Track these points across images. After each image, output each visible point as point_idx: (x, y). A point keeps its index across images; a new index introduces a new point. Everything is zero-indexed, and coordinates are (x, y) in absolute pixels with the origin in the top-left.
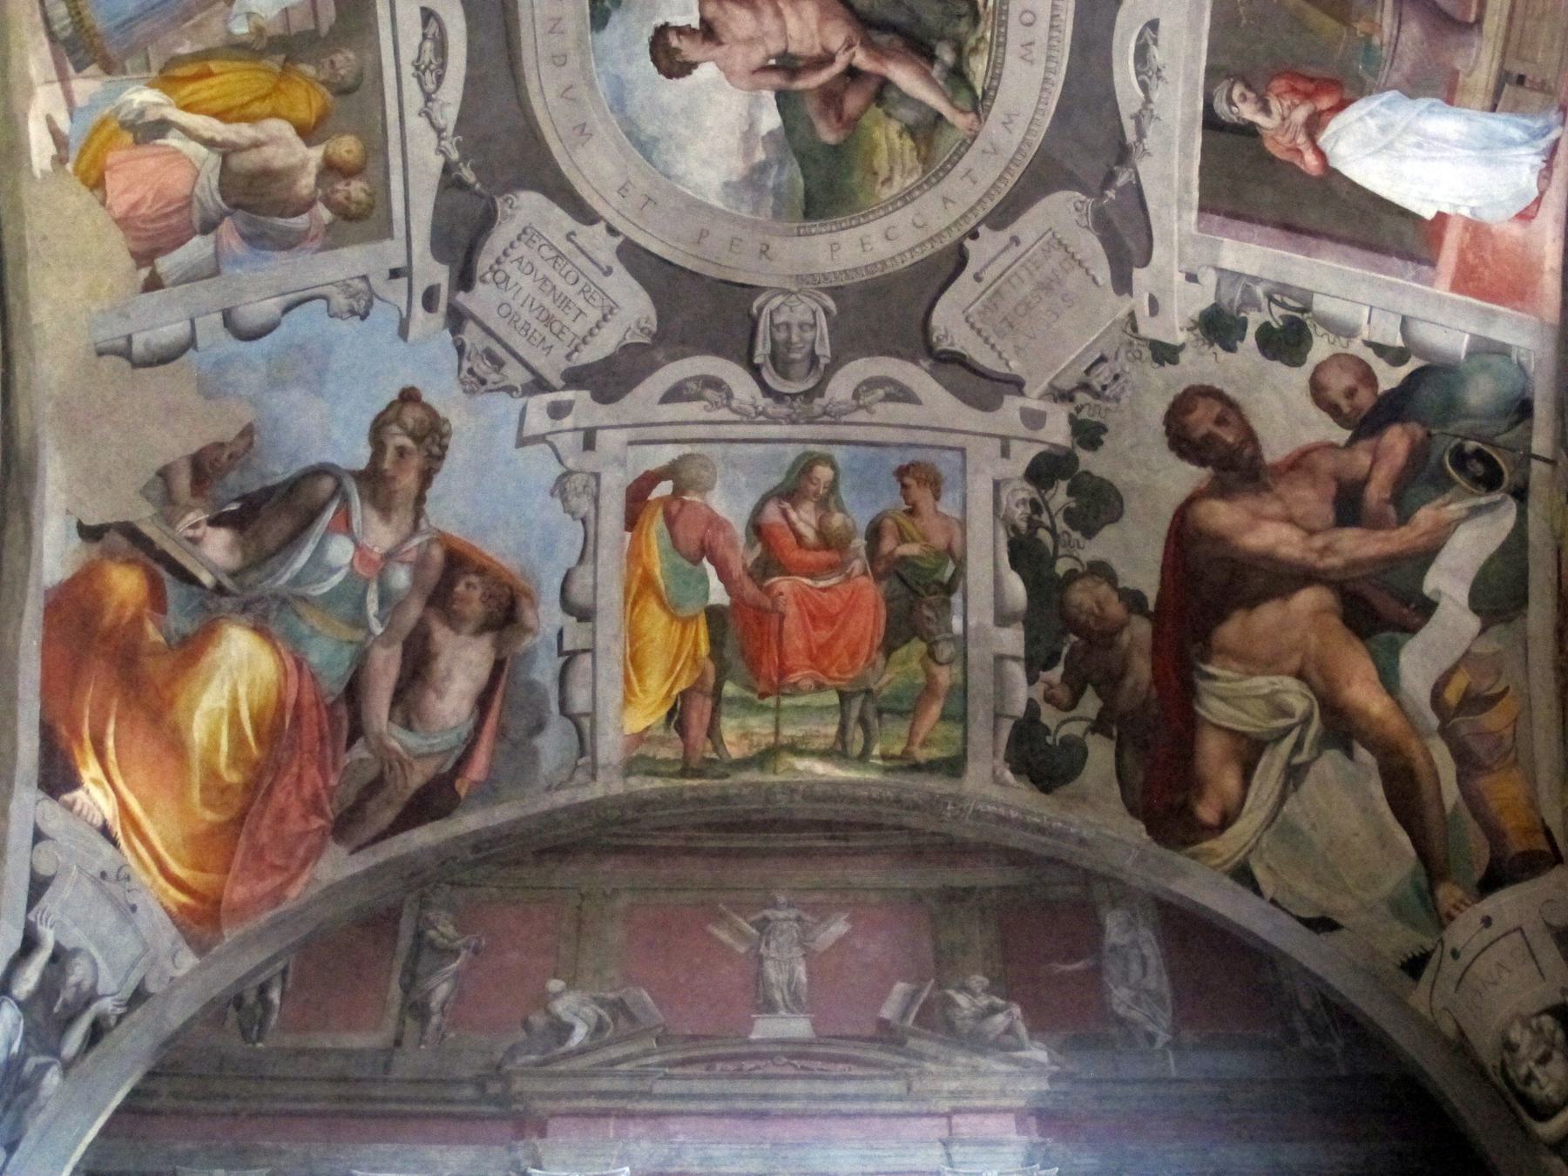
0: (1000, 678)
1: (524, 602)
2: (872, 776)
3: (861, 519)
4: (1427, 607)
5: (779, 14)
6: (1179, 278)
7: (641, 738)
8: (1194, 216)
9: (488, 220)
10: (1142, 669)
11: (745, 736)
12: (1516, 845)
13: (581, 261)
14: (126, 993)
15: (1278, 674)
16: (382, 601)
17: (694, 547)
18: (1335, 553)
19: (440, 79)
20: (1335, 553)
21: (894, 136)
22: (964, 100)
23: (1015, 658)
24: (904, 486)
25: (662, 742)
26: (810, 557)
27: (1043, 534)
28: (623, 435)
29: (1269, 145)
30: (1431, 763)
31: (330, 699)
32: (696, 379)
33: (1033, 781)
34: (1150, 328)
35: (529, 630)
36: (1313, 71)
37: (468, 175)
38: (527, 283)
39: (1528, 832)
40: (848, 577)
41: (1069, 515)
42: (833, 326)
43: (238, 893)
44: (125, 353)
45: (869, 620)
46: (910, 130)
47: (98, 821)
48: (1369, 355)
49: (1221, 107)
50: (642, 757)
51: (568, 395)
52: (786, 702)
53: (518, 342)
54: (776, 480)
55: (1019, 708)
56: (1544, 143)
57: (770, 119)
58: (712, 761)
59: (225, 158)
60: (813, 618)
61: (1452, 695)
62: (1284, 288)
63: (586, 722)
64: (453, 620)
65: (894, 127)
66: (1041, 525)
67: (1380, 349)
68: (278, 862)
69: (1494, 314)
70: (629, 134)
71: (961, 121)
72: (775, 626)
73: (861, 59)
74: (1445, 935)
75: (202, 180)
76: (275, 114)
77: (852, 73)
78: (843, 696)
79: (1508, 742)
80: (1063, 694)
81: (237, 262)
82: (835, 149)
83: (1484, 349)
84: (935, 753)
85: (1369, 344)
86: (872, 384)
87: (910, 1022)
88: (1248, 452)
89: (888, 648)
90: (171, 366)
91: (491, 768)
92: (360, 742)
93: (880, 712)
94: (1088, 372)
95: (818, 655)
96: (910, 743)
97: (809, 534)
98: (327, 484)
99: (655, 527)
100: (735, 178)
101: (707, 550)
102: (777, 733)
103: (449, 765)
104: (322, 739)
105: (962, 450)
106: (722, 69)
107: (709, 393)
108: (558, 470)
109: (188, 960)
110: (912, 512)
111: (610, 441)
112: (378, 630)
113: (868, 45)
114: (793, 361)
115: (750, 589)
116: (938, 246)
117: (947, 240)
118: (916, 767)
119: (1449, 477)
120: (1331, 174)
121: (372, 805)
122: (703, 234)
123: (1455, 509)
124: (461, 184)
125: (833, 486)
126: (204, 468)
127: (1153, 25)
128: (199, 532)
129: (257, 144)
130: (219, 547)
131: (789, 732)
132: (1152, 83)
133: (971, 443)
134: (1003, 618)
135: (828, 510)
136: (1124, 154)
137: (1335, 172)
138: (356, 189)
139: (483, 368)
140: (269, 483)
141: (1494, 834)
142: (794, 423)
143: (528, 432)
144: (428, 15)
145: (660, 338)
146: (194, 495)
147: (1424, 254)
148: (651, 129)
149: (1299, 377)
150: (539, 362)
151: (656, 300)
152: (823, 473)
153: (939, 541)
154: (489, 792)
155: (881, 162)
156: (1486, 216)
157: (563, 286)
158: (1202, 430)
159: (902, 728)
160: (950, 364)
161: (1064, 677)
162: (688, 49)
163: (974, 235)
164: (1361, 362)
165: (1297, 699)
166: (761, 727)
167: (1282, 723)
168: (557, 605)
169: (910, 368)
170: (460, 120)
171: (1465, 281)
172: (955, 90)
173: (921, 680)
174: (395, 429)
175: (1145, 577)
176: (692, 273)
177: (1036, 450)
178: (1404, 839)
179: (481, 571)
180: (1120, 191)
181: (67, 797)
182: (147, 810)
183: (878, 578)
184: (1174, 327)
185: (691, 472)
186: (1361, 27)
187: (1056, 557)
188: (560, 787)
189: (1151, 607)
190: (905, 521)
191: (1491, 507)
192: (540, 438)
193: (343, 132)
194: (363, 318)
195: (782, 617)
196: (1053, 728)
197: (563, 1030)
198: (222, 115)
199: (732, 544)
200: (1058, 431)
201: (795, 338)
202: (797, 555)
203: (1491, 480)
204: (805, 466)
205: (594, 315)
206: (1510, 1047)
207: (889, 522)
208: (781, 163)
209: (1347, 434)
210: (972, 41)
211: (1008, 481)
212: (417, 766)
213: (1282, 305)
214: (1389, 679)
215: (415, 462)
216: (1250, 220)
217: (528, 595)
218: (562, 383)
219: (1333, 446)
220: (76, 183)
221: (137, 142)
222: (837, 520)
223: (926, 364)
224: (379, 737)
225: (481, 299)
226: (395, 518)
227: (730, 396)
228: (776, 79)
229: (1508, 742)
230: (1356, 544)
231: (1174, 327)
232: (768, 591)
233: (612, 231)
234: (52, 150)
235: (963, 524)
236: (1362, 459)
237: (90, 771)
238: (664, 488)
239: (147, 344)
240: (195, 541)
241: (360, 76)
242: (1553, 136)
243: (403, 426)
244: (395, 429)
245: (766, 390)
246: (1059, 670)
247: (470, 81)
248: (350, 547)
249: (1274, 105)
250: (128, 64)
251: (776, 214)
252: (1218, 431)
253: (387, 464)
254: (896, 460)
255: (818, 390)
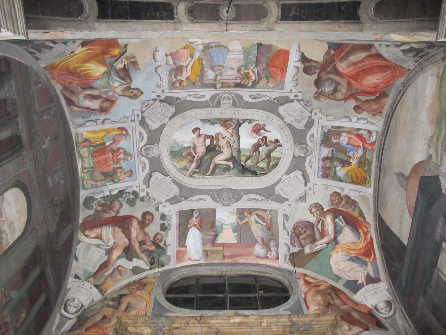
0: (100, 193)
1: (105, 113)
2: (80, 175)
3: (123, 165)
4: (131, 260)
5: (202, 146)
6: (169, 210)
7: (82, 135)
8: (179, 210)
9: (171, 104)
10: (107, 216)
11: (84, 152)
12: (103, 288)
13: (163, 118)
14: (39, 57)
15: (114, 239)
16: (107, 91)
17: (115, 139)
18: (134, 243)
19: (194, 97)
20: (134, 243)
21: (184, 164)
22: (191, 174)
23: (104, 194)
24: (129, 171)
25: (81, 139)
26: (115, 158)
27: (125, 195)
28: (134, 126)
29: (191, 220)
30: (109, 269)
31: (90, 84)
32: (143, 136)
33: (84, 202)
34: (160, 206)
35: (100, 114)
36: (202, 224)
37: (178, 101)
38: (159, 110)
39: (105, 288)
40: (112, 165)
41: (129, 199)
42: (153, 157)
43: (55, 72)
44: (156, 51)
45: (106, 169)
46: (185, 166)
47: (75, 51)
48: (164, 240)
49: (195, 212)
50: (78, 136)
51: (140, 117)
52: (90, 158)
53: (150, 109)
54: (127, 150)
55: (96, 197)
56: (200, 259)
57: (186, 145)
58: (79, 148)
59: (186, 66)
60: (105, 160)
61: (120, 268)
62: (171, 225)
63: (84, 125)
64: (102, 102)
65: (186, 164)
66: (126, 195)
67: (165, 242)
68: (60, 78)
69: (175, 258)
70: (183, 125)
71: (188, 174)
72: (103, 154)
73: (196, 158)
74: (85, 281)
75: (182, 63)
76: (191, 73)
77: (194, 157)
78: (93, 167)
79: (116, 280)
80: (100, 204)
81: (168, 68)
82: (182, 155)
83: (169, 258)
84: (85, 184)
85: (166, 240)
86: (145, 164)
87: (54, 203)
88: (146, 225)
89: (102, 173)
90: (153, 58)
91: (75, 111)
92: (82, 90)
93: (91, 174)
94: (152, 198)
95: (99, 162)
96: (86, 180)
97: (119, 157)
98: (129, 81)
99: (118, 132)
100: (176, 140)
101: (115, 141)
102: (85, 157)
103: (76, 104)
104: (83, 83)
105: (136, 180)
106: (194, 138)
107: (141, 138)
108: (128, 116)
109: (43, 66)
110: (125, 173)
111: (133, 124)
112: (102, 91)
113: (198, 159)
114: (147, 151)
115: (109, 149)
116: (168, 172)
117: (169, 173)
118: (83, 182)
119: (150, 257)
120: (188, 229)
121: (69, 93)
122: (167, 136)
123: (146, 260)
124: (177, 100)
125: (127, 160)
126: (135, 63)
127: (205, 200)
128: (123, 63)
129: (187, 71)
130: (119, 65)
131: (85, 159)
132: (197, 201)
133: (137, 181)
134: (110, 191)
135: (124, 159)
136: (186, 198)
137: (189, 230)
138: (178, 85)
139: (146, 104)
140: (130, 73)
141: (104, 283)
142: (137, 152)
143: (134, 111)
144: (204, 96)
145: (150, 130)
146: (130, 62)
147: (180, 245)
148: (184, 127)
149: (159, 231)
150: (146, 112)
151: (156, 129)
152: (129, 158)
153: (121, 178)
154: (71, 111)
155: (180, 162)
156: (188, 253)
157: (159, 115)
158: (147, 217)
159: (89, 178)
160: (150, 176)
161: (102, 203)
162: (197, 133)
163: (170, 177)
164: (163, 239)
165: (111, 243)
166: (86, 154)
167: (106, 242)
168: (105, 118)
169: (148, 169)
170: (187, 100)
171: (178, 252)
172: (192, 172)
173: (97, 180)
174: (137, 91)
175: (122, 213)
176: (160, 135)
177: (139, 192)
178: (97, 269)
179: (111, 106)
180: (180, 199)
181: (80, 46)
182: (75, 58)
183: (113, 170)
184: (161, 210)
185: (128, 137)
186: (210, 230)
187: (122, 198)
188: (73, 123)
189: (118, 215)
190: (123, 172)
191: (148, 265)
192: (133, 113)
193: (187, 83)
194: (156, 86)
195: (105, 155)
196: (94, 203)
197: (43, 144)
198: (192, 66)
199: (116, 145)
200: (142, 194)
201: (151, 151)
202: (115, 155)
203: (152, 264)
204: (130, 155)
205: (154, 120)
206: (73, 300)
207: (123, 170)
208: (179, 147)
209: (152, 240)
210: (200, 174)
211: (132, 188)
212: (76, 99)
213: (168, 226)
214: (119, 257)
215: (131, 95)
216: (180, 218)
217: (106, 113)
218: (143, 116)
219: (150, 238)
220: (186, 45)
221: (190, 54)
222: (122, 161)
223: (149, 172)
224: (82, 92)
225: (158, 103)
226: (122, 92)
227: (141, 142)
228: (192, 146)
229: (116, 280)
230: (136, 246)
231: (162, 210)
232: (109, 152)
233: (168, 122)
234: (192, 42)
235: (124, 182)
236: (149, 243)
237: (84, 49)
238: (125, 133)
239: (156, 54)
240: (122, 62)
241: (196, 86)
242: (201, 260)
243: (137, 92)
244: (137, 91)
245: (142, 148)
246: (104, 202)
247: (193, 102)
248: (117, 86)
249: (197, 219)
250: (203, 53)
251: (171, 147)
252: (147, 220)
253: (131, 90)
254: (133, 169)
255: (143, 155)
